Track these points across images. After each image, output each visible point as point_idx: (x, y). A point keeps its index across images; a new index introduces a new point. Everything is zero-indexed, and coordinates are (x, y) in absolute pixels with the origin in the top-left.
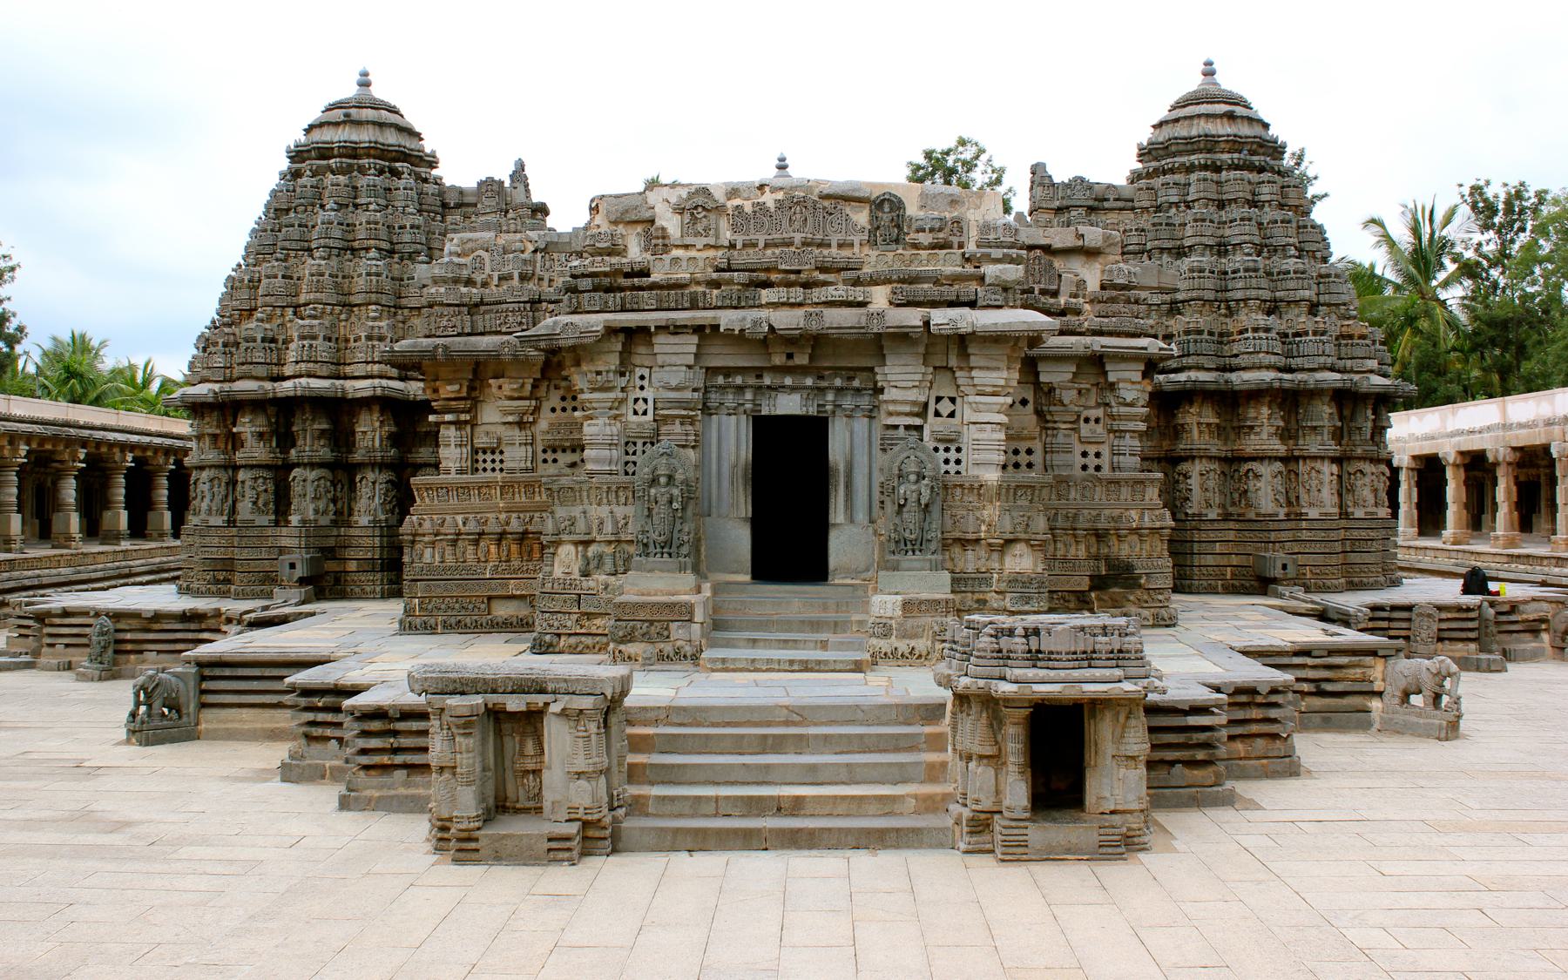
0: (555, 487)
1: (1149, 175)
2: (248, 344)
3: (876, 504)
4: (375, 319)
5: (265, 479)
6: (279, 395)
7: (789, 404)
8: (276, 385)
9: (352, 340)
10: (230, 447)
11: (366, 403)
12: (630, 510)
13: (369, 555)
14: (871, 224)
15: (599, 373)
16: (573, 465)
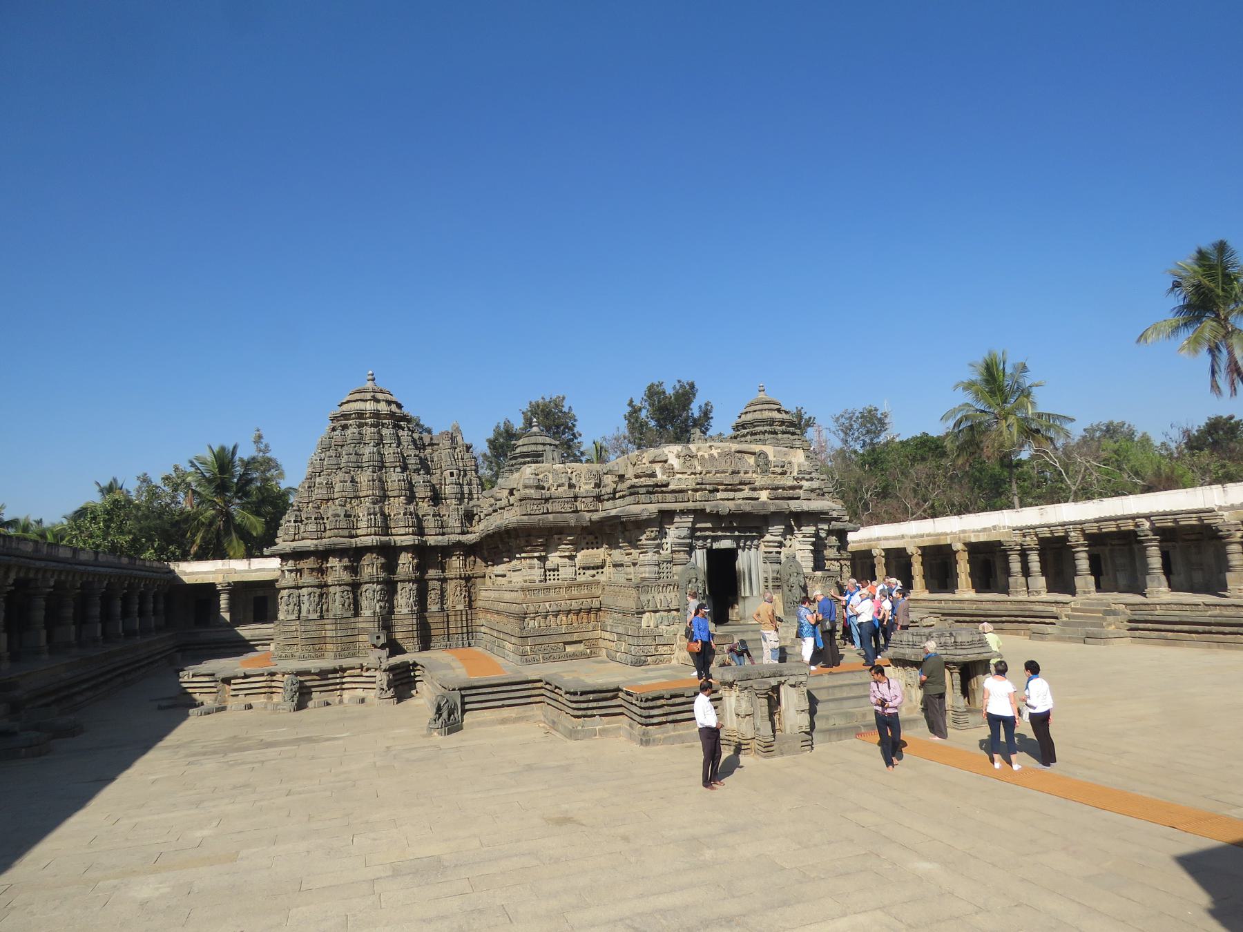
0: (641, 586)
1: (744, 436)
2: (337, 518)
3: (762, 587)
4: (406, 504)
5: (348, 591)
6: (359, 545)
7: (726, 544)
8: (357, 539)
9: (392, 515)
10: (319, 575)
11: (406, 549)
12: (673, 595)
13: (411, 629)
14: (756, 462)
15: (652, 532)
16: (594, 576)
